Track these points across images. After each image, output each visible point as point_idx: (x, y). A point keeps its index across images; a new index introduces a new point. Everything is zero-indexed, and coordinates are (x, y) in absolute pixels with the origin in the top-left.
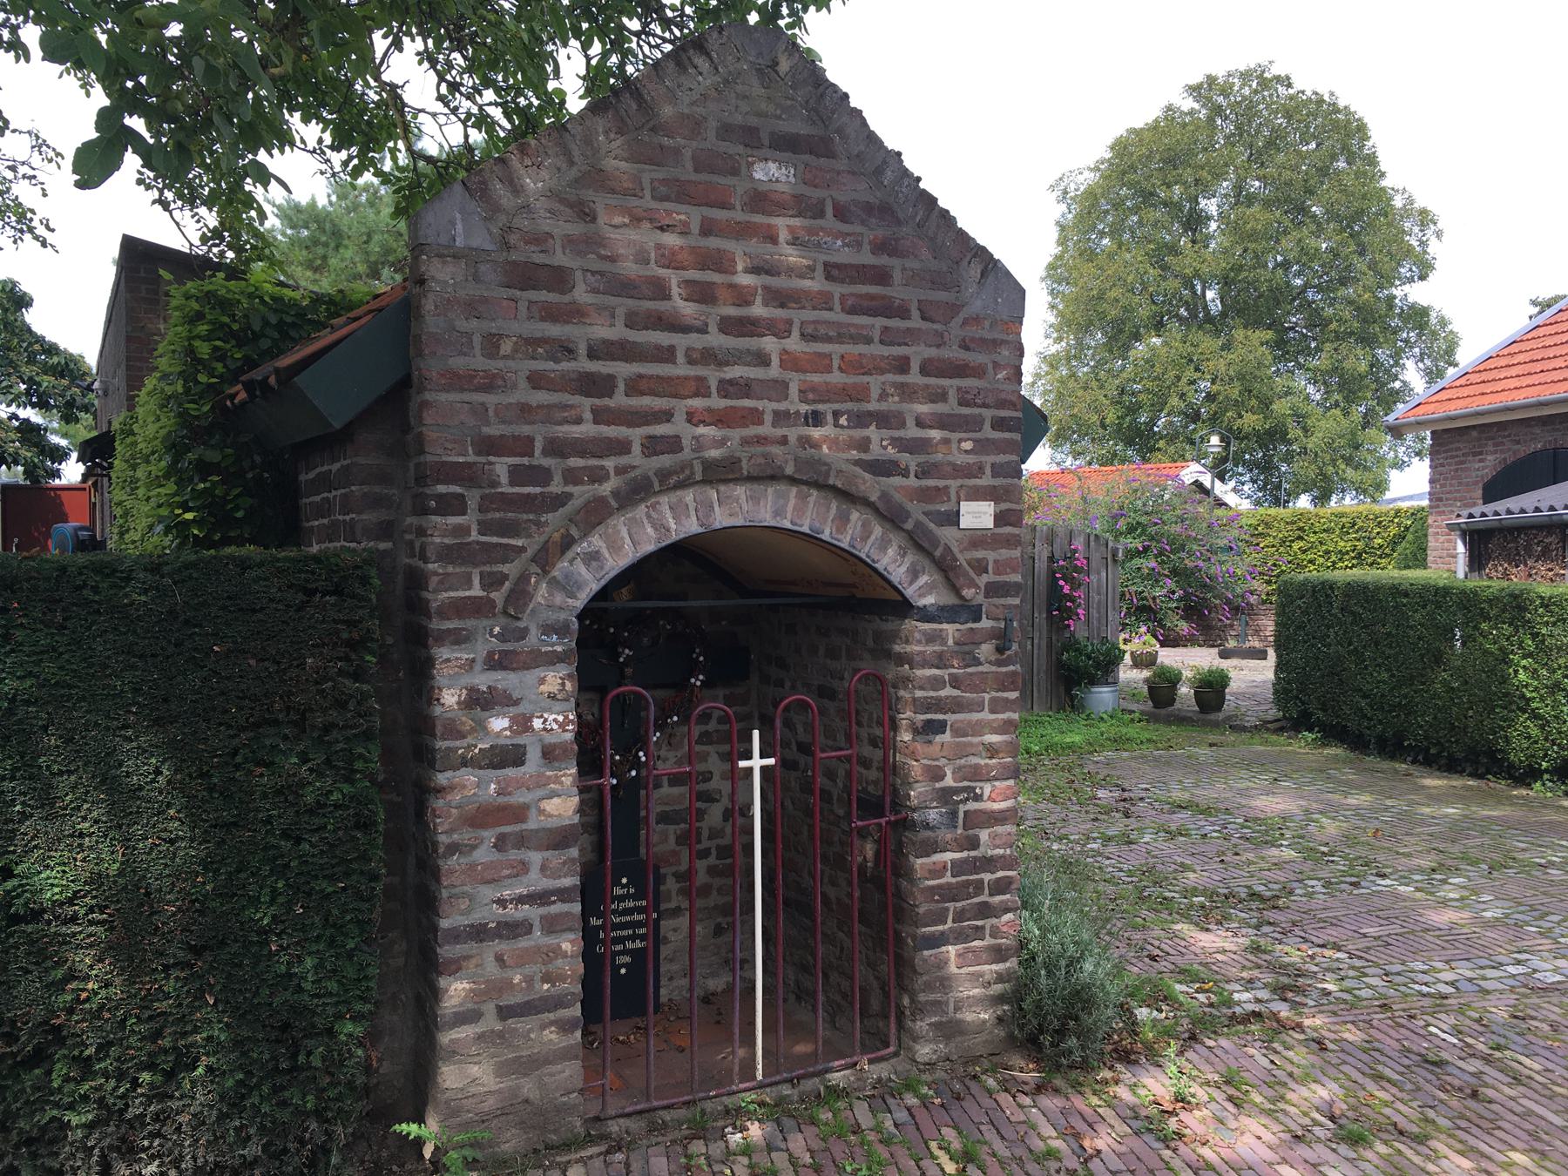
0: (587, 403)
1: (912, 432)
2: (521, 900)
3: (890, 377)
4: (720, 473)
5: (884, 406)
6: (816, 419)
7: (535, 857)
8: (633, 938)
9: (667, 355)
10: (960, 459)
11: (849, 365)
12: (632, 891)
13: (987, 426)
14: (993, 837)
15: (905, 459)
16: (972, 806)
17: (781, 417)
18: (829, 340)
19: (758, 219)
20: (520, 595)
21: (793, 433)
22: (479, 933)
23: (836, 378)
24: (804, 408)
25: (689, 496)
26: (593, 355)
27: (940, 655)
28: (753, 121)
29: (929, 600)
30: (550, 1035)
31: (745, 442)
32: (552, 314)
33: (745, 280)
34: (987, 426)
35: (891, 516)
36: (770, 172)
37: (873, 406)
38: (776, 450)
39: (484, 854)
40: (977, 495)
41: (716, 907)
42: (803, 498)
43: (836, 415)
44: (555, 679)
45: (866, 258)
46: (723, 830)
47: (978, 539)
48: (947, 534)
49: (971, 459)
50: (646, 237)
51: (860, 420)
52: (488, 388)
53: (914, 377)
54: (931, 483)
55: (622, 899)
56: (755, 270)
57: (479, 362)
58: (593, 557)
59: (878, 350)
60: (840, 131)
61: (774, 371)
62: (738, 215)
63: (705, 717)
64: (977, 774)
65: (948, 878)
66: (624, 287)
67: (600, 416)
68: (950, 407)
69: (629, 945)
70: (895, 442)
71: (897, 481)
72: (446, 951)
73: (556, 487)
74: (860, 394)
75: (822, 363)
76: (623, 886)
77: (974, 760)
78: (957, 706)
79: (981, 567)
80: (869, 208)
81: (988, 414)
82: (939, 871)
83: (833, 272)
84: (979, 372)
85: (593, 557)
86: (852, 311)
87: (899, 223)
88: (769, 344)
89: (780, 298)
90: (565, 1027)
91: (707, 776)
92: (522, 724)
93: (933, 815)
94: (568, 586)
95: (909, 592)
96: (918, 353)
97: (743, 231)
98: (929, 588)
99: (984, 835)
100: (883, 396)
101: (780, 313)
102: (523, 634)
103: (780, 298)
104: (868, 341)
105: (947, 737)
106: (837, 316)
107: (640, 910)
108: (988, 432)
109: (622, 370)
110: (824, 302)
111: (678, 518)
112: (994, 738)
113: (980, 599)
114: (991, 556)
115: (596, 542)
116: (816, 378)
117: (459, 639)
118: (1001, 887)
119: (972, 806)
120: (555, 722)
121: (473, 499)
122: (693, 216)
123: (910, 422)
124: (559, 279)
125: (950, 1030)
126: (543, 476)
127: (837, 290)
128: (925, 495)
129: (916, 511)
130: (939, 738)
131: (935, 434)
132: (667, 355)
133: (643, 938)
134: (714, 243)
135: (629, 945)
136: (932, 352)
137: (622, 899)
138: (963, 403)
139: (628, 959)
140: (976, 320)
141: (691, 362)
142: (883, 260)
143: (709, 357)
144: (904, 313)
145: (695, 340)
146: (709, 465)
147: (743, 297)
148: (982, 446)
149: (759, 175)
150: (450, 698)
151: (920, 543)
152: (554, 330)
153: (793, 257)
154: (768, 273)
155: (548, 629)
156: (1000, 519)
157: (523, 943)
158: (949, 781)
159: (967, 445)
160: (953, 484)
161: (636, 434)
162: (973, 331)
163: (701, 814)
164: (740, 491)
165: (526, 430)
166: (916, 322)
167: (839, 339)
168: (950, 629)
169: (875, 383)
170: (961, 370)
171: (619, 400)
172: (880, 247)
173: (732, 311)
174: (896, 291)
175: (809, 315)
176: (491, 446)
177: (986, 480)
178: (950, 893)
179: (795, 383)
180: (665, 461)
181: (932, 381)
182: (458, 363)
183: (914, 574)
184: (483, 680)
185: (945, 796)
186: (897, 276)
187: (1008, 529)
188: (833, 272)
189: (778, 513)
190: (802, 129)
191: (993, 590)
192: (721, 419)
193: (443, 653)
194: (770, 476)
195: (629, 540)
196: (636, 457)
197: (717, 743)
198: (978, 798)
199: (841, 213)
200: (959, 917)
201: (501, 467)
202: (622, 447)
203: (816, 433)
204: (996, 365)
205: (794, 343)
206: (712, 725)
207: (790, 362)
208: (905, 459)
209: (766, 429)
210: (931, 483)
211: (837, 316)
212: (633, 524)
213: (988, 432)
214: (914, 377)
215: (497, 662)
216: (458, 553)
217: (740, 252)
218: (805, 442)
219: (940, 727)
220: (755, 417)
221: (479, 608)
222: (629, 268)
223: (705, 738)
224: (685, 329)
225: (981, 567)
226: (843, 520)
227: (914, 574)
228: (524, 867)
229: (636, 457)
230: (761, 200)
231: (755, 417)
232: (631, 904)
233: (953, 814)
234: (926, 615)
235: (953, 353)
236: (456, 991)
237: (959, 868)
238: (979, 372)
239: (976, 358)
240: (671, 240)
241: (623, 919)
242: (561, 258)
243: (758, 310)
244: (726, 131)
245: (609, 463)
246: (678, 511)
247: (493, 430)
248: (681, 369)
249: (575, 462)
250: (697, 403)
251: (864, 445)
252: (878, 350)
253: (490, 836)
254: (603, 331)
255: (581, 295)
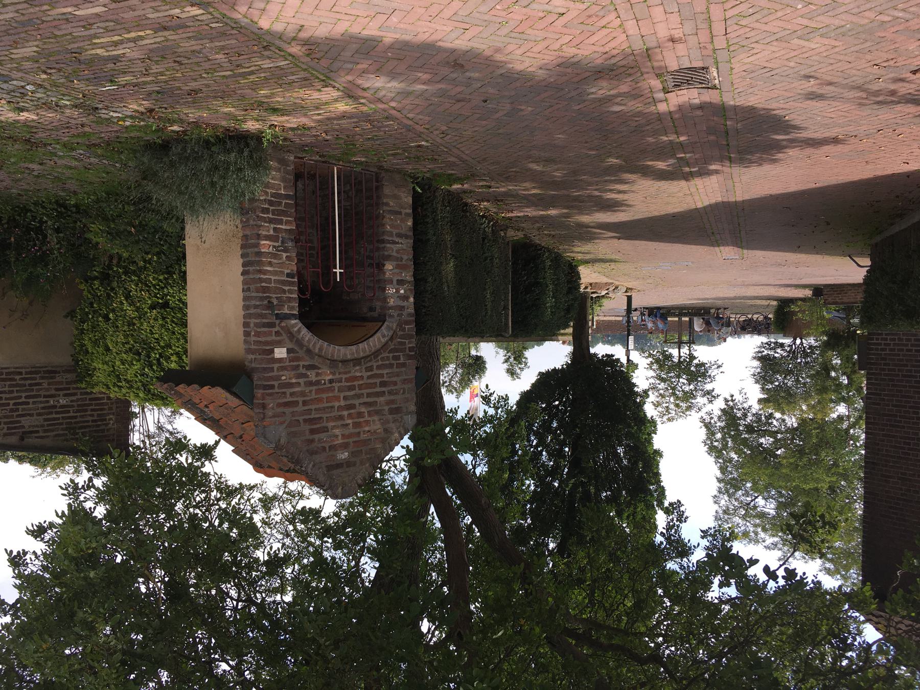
0: (385, 379)
1: (301, 381)
2: (398, 243)
3: (308, 398)
4: (357, 361)
5: (311, 388)
6: (331, 381)
7: (394, 254)
9: (369, 395)
10: (285, 372)
11: (319, 400)
13: (276, 386)
14: (268, 231)
15: (304, 371)
16: (276, 244)
17: (340, 381)
18: (328, 407)
19: (346, 441)
20: (400, 325)
21: (337, 376)
22: (407, 237)
23: (324, 396)
24: (334, 384)
25: (362, 355)
26: (384, 392)
27: (289, 302)
28: (347, 469)
29: (293, 322)
30: (391, 204)
31: (350, 372)
32: (392, 402)
33: (350, 421)
34: (276, 386)
35: (309, 352)
36: (344, 455)
37: (314, 388)
38: (342, 370)
39: (405, 257)
40: (280, 360)
42: (333, 356)
43: (325, 384)
44: (392, 302)
45: (316, 437)
47: (279, 344)
48: (291, 346)
49: (281, 373)
50: (373, 427)
51: (318, 383)
52: (405, 380)
53: (300, 399)
54: (295, 363)
56: (347, 425)
57: (406, 386)
58: (384, 336)
59: (313, 407)
60: (324, 475)
61: (342, 395)
62: (351, 440)
64: (275, 256)
65: (285, 219)
66: (377, 412)
67: (382, 376)
68: (288, 391)
70: (307, 376)
71: (307, 363)
72: (411, 234)
73: (391, 355)
74: (318, 391)
75: (329, 400)
77: (275, 261)
78: (283, 283)
79: (277, 333)
80: (316, 453)
81: (276, 390)
82: (287, 223)
83: (325, 430)
84: (279, 405)
85: (384, 336)
86: (321, 418)
87: (307, 451)
88: (343, 403)
89: (341, 418)
90: (387, 204)
92: (398, 291)
93: (290, 244)
94: (389, 328)
95: (300, 325)
96: (300, 408)
97: (350, 436)
98: (294, 326)
99: (272, 232)
100: (311, 391)
101: (340, 413)
102: (398, 315)
103: (341, 418)
104: (316, 409)
105: (286, 271)
106: (325, 416)
108: (276, 383)
109: (378, 389)
110: (329, 419)
111: (365, 348)
112: (269, 268)
113: (277, 322)
114: (274, 338)
115: (383, 340)
116: (330, 395)
117: (409, 315)
118: (265, 211)
119: (276, 244)
120: (391, 291)
121: (407, 351)
122: (363, 436)
123: (302, 384)
124: (391, 412)
125: (283, 162)
126: (396, 358)
127: (324, 424)
128: (297, 359)
129: (301, 353)
130: (289, 271)
131: (294, 381)
132: (369, 395)
134: (357, 430)
136: (295, 409)
138: (284, 393)
140: (281, 423)
141: (363, 394)
142: (311, 437)
143: (358, 396)
144: (305, 421)
145: (361, 401)
146: (360, 364)
147: (350, 416)
148: (278, 378)
149: (346, 454)
150: (412, 300)
151: (299, 343)
152: (392, 397)
153: (337, 431)
154: (343, 425)
155: (393, 316)
156: (272, 351)
157: (397, 231)
158: (285, 255)
159: (284, 378)
160: (287, 364)
161: (375, 371)
162: (282, 419)
164: (349, 357)
165: (398, 370)
166: (301, 419)
167: (324, 408)
168: (286, 311)
169: (314, 396)
170: (286, 404)
171: (378, 381)
172: (312, 441)
173: (352, 411)
174: (306, 427)
175: (332, 415)
176: (404, 365)
177: (276, 366)
178: (283, 213)
179: (336, 393)
180: (369, 364)
181: (295, 399)
182: (410, 386)
183: (299, 331)
184: (405, 304)
185: (286, 250)
186: (307, 432)
187: (268, 348)
188: (325, 430)
189: (339, 350)
190: (335, 472)
191: (272, 325)
192: (355, 378)
193: (413, 311)
194: (344, 362)
195: (376, 341)
196: (375, 365)
198: (274, 247)
199: (324, 448)
200: (280, 204)
201: (402, 360)
202: (379, 367)
203: (330, 377)
204: (273, 408)
205: (336, 404)
207: (337, 398)
208: (304, 371)
209: (344, 376)
210: (295, 363)
211: (325, 416)
212: (375, 346)
213: (276, 383)
214: (300, 399)
215: (402, 308)
216: (411, 337)
217: (351, 430)
218: (334, 374)
219: (288, 275)
220: (347, 380)
221: (407, 323)
222: (376, 418)
224: (364, 403)
225: (277, 333)
226: (321, 349)
227: (299, 331)
228: (398, 252)
229: (375, 365)
230: (345, 446)
231: (347, 380)
233: (283, 242)
234: (293, 316)
235: (288, 410)
236: (410, 223)
237: (280, 222)
238: (279, 405)
239: (281, 410)
240: (367, 429)
242: (390, 417)
243: (345, 413)
244: (354, 464)
245: (380, 363)
246: (364, 350)
247: (403, 369)
248: (365, 391)
249: (387, 362)
250: (361, 382)
251: (317, 374)
252: (313, 407)
253: (404, 262)
254: (382, 399)
255: (386, 408)
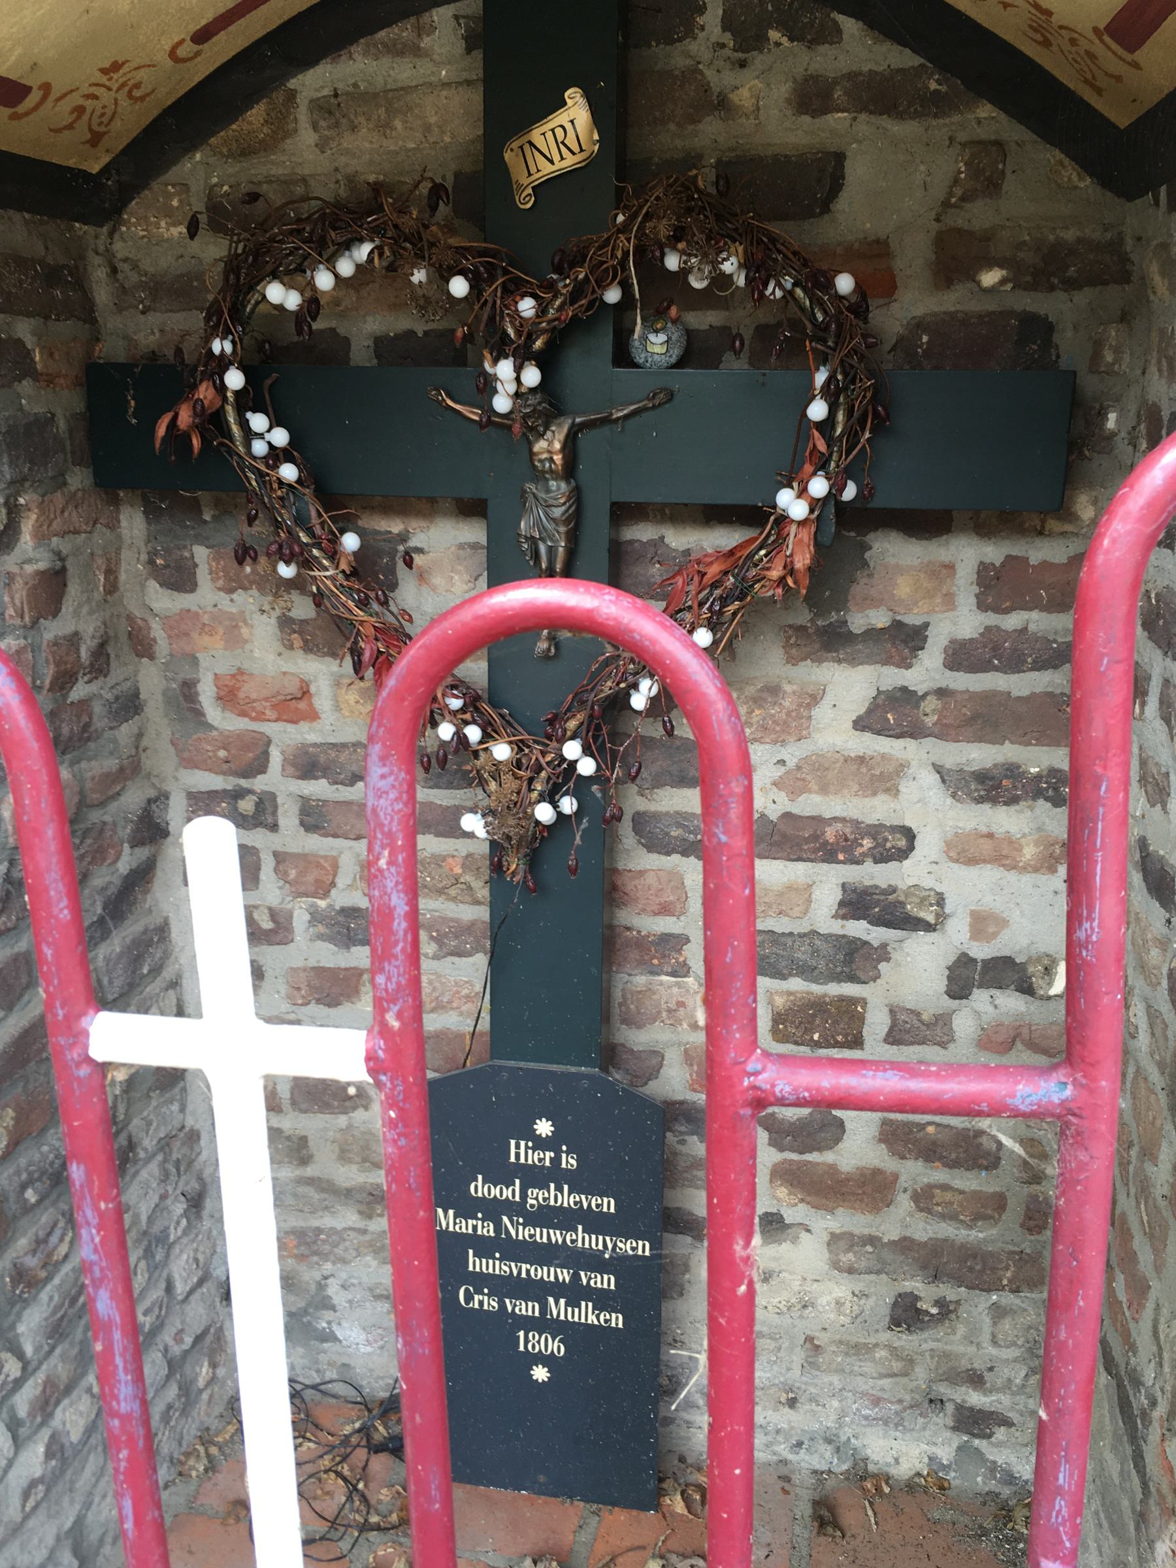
8: (575, 1294)
12: (569, 1162)
41: (905, 1245)
46: (943, 1020)
55: (534, 1177)
63: (905, 640)
69: (558, 1309)
76: (541, 1144)
91: (897, 843)
107: (595, 1223)
133: (602, 1301)
135: (558, 1309)
137: (534, 1177)
139: (555, 1347)
163: (855, 960)
197: (944, 732)
206: (926, 672)
223: (892, 714)
232: (567, 1199)
241: (541, 1235)
